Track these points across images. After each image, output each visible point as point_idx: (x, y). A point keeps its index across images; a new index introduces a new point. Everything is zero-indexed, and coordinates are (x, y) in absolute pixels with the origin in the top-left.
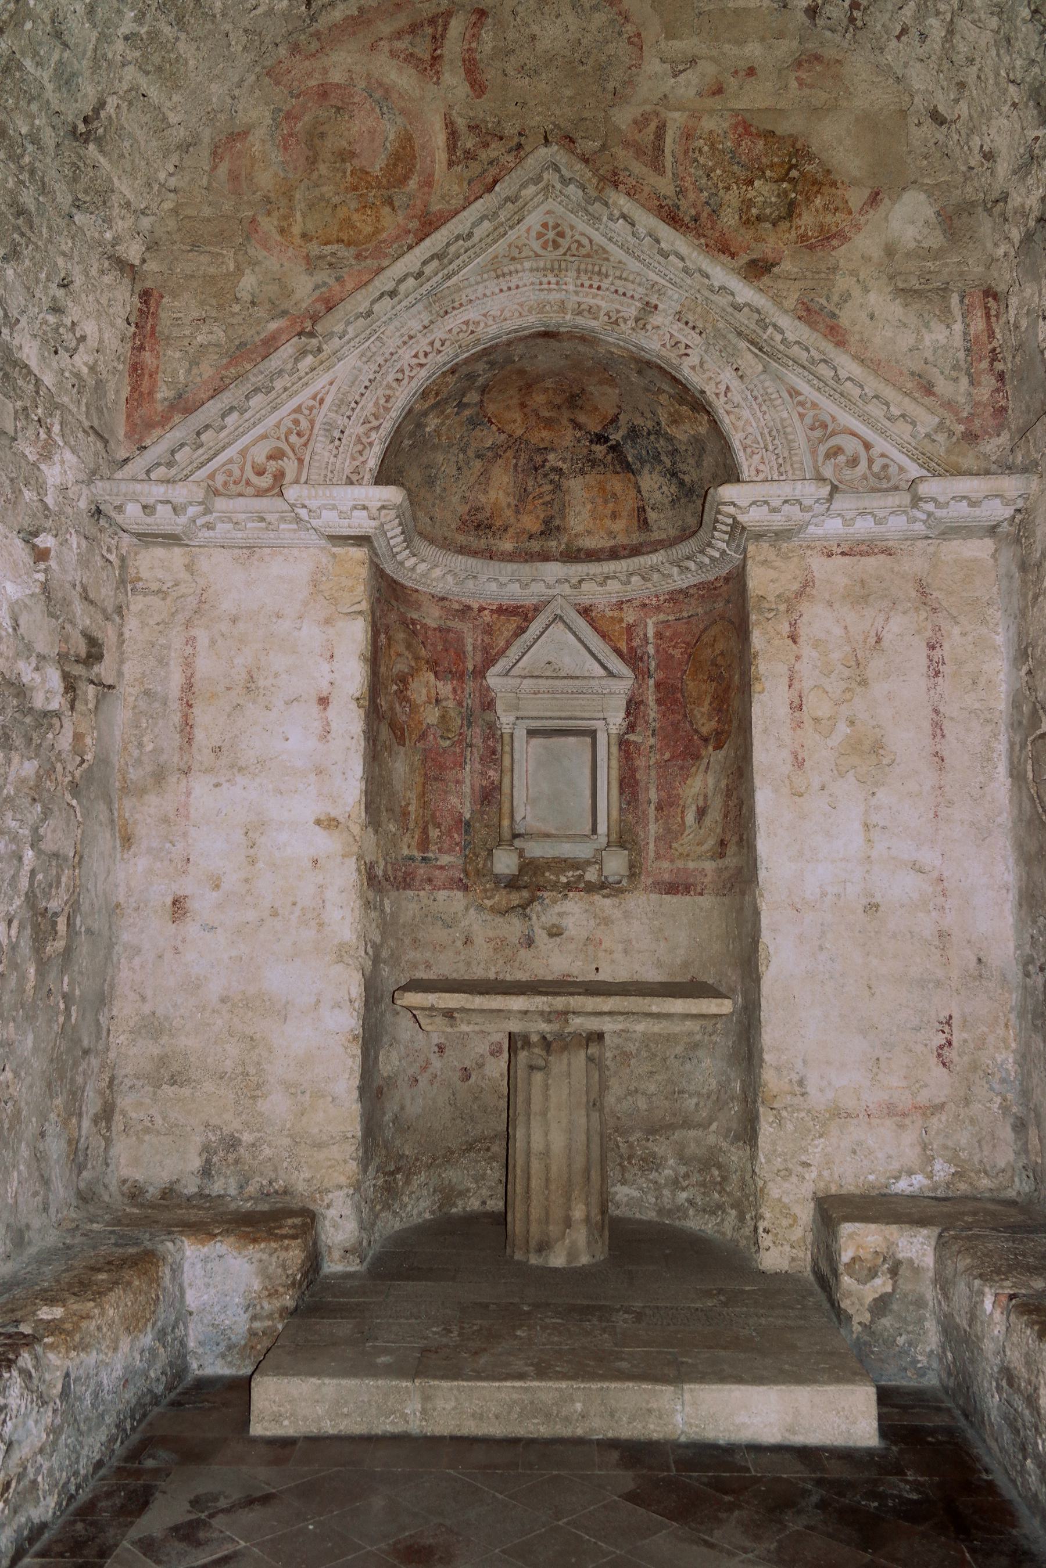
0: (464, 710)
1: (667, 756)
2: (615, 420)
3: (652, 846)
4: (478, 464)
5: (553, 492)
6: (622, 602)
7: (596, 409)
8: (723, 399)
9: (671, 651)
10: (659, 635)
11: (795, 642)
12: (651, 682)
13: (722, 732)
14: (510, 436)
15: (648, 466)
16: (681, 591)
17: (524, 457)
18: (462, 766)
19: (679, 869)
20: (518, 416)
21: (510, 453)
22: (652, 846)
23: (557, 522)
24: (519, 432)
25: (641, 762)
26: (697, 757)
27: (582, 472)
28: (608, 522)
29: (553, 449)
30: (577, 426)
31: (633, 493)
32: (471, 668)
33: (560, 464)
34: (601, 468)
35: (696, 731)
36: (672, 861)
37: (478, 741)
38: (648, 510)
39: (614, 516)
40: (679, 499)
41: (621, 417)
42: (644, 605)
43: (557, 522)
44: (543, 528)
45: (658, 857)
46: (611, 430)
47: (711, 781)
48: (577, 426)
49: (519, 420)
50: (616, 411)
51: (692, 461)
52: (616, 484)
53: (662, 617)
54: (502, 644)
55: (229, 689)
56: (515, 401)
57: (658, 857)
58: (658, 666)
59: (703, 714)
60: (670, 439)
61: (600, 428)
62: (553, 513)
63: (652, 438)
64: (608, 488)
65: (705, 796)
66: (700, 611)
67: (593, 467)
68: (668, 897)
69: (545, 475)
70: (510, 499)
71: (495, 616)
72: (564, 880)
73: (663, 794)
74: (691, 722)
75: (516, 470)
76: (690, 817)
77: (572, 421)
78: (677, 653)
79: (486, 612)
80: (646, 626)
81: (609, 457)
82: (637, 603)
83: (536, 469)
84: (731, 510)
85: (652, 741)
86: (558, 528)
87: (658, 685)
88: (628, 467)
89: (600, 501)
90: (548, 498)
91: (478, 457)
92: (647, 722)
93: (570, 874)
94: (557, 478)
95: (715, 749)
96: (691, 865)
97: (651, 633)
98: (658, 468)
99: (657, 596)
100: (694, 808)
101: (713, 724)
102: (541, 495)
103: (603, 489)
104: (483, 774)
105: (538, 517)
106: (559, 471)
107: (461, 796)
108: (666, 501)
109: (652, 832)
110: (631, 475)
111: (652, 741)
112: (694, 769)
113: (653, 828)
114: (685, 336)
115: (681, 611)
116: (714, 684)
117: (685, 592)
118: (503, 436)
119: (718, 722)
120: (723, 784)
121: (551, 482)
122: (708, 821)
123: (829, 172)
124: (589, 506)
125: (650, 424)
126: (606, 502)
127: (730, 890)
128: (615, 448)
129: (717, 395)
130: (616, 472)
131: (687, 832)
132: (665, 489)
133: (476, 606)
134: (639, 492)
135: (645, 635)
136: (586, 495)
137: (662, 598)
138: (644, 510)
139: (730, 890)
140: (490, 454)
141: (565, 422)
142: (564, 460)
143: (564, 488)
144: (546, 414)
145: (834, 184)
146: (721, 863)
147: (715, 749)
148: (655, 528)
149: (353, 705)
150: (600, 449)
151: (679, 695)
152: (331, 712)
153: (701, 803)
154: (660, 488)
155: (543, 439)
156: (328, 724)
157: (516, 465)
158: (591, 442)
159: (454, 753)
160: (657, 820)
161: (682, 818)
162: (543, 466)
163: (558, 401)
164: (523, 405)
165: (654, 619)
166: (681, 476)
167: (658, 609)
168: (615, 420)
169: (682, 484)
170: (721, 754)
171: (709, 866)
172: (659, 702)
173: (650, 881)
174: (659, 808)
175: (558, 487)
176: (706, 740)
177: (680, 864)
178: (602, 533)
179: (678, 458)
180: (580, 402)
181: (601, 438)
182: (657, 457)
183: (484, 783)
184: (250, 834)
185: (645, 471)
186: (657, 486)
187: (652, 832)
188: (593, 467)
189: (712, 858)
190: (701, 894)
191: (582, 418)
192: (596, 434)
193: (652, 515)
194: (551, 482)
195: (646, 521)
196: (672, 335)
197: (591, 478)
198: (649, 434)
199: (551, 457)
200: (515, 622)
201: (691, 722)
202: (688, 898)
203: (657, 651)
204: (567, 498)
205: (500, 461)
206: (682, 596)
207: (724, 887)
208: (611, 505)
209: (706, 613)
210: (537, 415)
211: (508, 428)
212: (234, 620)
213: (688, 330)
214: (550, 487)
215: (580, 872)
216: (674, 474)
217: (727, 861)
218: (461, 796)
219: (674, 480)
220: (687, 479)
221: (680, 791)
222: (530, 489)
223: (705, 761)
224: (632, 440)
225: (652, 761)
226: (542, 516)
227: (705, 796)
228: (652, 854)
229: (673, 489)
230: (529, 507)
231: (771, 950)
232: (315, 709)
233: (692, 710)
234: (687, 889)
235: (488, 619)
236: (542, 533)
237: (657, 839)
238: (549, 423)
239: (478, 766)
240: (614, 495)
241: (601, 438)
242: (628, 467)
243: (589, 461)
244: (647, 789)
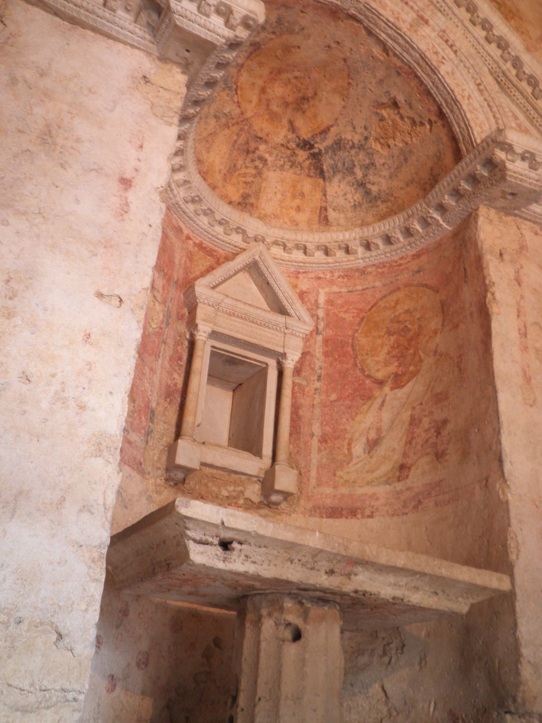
0: (166, 309)
1: (333, 397)
2: (325, 131)
3: (313, 473)
4: (212, 122)
5: (255, 176)
6: (299, 273)
7: (315, 116)
8: (466, 101)
9: (342, 315)
10: (330, 302)
11: (519, 284)
12: (320, 338)
13: (404, 374)
14: (242, 113)
15: (339, 176)
16: (357, 270)
17: (242, 140)
18: (157, 356)
19: (343, 495)
20: (255, 99)
21: (236, 129)
22: (313, 473)
23: (252, 200)
24: (249, 114)
25: (305, 401)
26: (368, 397)
27: (282, 167)
28: (293, 213)
29: (266, 142)
30: (293, 128)
31: (319, 195)
32: (176, 278)
33: (267, 156)
34: (298, 170)
35: (368, 376)
36: (335, 487)
37: (170, 342)
38: (330, 210)
39: (298, 209)
40: (360, 205)
41: (332, 129)
42: (319, 278)
43: (252, 200)
44: (240, 200)
45: (319, 484)
46: (318, 140)
47: (386, 416)
48: (293, 128)
49: (254, 103)
50: (330, 123)
51: (385, 173)
52: (307, 185)
53: (335, 289)
54: (198, 273)
55: (20, 131)
56: (260, 83)
57: (319, 484)
58: (327, 326)
59: (377, 363)
60: (370, 155)
61: (309, 135)
62: (250, 193)
63: (353, 152)
64: (299, 187)
65: (379, 430)
66: (378, 284)
67: (291, 167)
68: (330, 521)
69: (253, 161)
70: (222, 167)
71: (196, 249)
72: (225, 493)
73: (328, 429)
74: (362, 370)
75: (233, 146)
76: (358, 449)
77: (291, 123)
78: (348, 317)
79: (191, 242)
80: (318, 294)
81: (307, 162)
82: (313, 275)
83: (248, 152)
84: (500, 155)
85: (317, 385)
86: (252, 205)
87: (326, 341)
88: (321, 174)
89: (289, 195)
90: (249, 179)
91: (216, 117)
92: (313, 369)
93: (231, 488)
94: (261, 166)
95: (392, 389)
96: (360, 491)
97: (322, 299)
98: (350, 178)
99: (332, 272)
100: (364, 440)
101: (392, 368)
102: (245, 175)
103: (294, 186)
104: (170, 374)
105: (238, 191)
106: (264, 161)
107: (152, 384)
108: (348, 205)
109: (314, 461)
110: (321, 181)
111: (317, 385)
112: (366, 407)
113: (315, 458)
114: (443, 50)
115: (355, 285)
116: (393, 339)
117: (363, 272)
118: (238, 111)
119: (400, 365)
120: (406, 416)
121: (256, 167)
122: (381, 450)
123: (518, 10)
124: (279, 196)
125: (357, 138)
126: (294, 197)
127: (416, 507)
128: (316, 156)
129: (463, 97)
130: (309, 176)
131: (354, 461)
132: (349, 196)
133: (186, 231)
134: (325, 195)
135: (316, 301)
136: (279, 187)
137: (336, 274)
138: (326, 209)
139: (416, 507)
140: (223, 120)
141: (285, 122)
142: (271, 153)
143: (264, 176)
144: (274, 108)
145: (521, 18)
146: (399, 486)
147: (392, 389)
148: (335, 224)
149: (157, 198)
150: (302, 155)
151: (349, 349)
152: (131, 196)
153: (373, 435)
154: (345, 194)
155: (262, 130)
156: (127, 204)
157: (236, 141)
158: (298, 145)
159: (154, 342)
160: (320, 450)
161: (349, 449)
162: (254, 152)
163: (290, 99)
164: (263, 90)
165: (327, 290)
166: (369, 186)
167: (332, 282)
168: (325, 131)
169: (368, 193)
170: (401, 393)
171: (382, 490)
172: (326, 354)
173: (310, 505)
174: (324, 440)
175: (259, 173)
176: (381, 383)
177: (344, 490)
178: (286, 220)
179: (371, 171)
180: (306, 106)
181: (306, 145)
182: (350, 171)
183: (169, 382)
184: (13, 284)
185: (336, 179)
186: (341, 193)
187: (314, 461)
188: (291, 167)
189: (387, 483)
190: (371, 516)
191: (299, 123)
192: (304, 140)
193: (332, 215)
194: (256, 167)
195: (326, 219)
196: (434, 46)
197: (289, 175)
198: (353, 147)
199: (262, 147)
200: (209, 261)
201: (362, 370)
202: (354, 521)
203: (327, 314)
204: (264, 185)
205: (227, 131)
206: (357, 274)
207: (404, 506)
208: (297, 202)
209: (384, 285)
210: (268, 105)
211: (243, 105)
212: (42, 74)
213: (445, 46)
214: (254, 172)
215: (240, 488)
216: (362, 185)
217: (409, 482)
218: (152, 384)
219: (361, 190)
220: (374, 189)
221: (348, 427)
222: (239, 167)
223: (379, 401)
224: (334, 151)
225: (317, 401)
226: (241, 191)
227: (379, 430)
228: (313, 481)
229: (358, 197)
230: (234, 180)
231: (520, 539)
232: (115, 186)
233: (363, 361)
234: (353, 513)
235: (191, 248)
236: (239, 204)
237: (320, 467)
238: (273, 117)
239: (167, 365)
240: (302, 195)
241: (306, 145)
242: (321, 174)
243: (290, 161)
244: (310, 424)
